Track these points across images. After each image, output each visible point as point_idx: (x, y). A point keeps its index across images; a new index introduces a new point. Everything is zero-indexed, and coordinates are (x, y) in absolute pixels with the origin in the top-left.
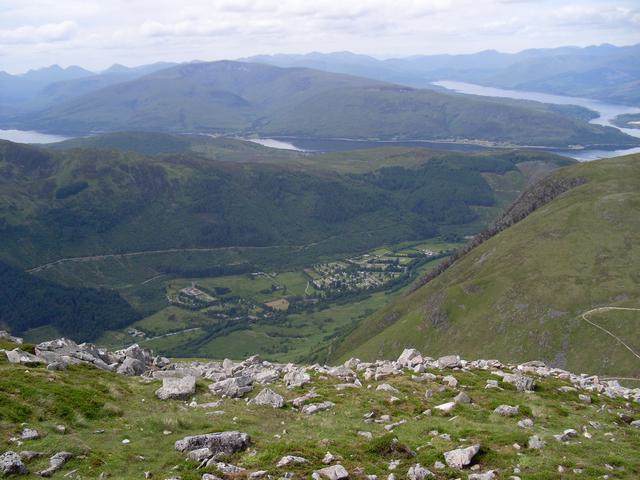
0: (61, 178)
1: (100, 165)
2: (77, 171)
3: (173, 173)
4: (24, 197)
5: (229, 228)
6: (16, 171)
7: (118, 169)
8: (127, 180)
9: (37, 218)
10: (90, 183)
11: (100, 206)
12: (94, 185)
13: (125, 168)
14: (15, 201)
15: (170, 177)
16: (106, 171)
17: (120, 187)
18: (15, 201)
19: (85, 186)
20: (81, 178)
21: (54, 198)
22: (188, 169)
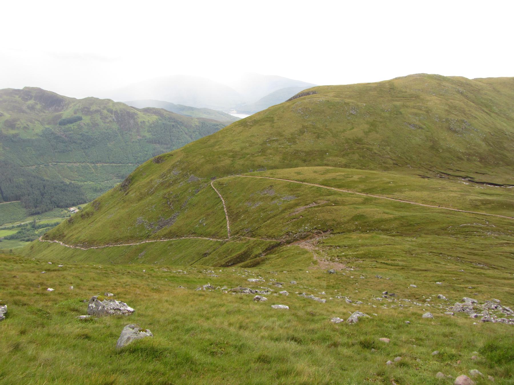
0: (67, 113)
1: (94, 108)
2: (78, 110)
3: (142, 117)
4: (36, 122)
6: (38, 107)
7: (105, 112)
8: (110, 119)
9: (41, 136)
10: (83, 118)
11: (87, 132)
12: (86, 119)
13: (110, 111)
14: (29, 123)
15: (140, 120)
16: (97, 111)
17: (105, 123)
18: (29, 123)
19: (80, 119)
20: (79, 114)
21: (58, 125)
22: (155, 116)
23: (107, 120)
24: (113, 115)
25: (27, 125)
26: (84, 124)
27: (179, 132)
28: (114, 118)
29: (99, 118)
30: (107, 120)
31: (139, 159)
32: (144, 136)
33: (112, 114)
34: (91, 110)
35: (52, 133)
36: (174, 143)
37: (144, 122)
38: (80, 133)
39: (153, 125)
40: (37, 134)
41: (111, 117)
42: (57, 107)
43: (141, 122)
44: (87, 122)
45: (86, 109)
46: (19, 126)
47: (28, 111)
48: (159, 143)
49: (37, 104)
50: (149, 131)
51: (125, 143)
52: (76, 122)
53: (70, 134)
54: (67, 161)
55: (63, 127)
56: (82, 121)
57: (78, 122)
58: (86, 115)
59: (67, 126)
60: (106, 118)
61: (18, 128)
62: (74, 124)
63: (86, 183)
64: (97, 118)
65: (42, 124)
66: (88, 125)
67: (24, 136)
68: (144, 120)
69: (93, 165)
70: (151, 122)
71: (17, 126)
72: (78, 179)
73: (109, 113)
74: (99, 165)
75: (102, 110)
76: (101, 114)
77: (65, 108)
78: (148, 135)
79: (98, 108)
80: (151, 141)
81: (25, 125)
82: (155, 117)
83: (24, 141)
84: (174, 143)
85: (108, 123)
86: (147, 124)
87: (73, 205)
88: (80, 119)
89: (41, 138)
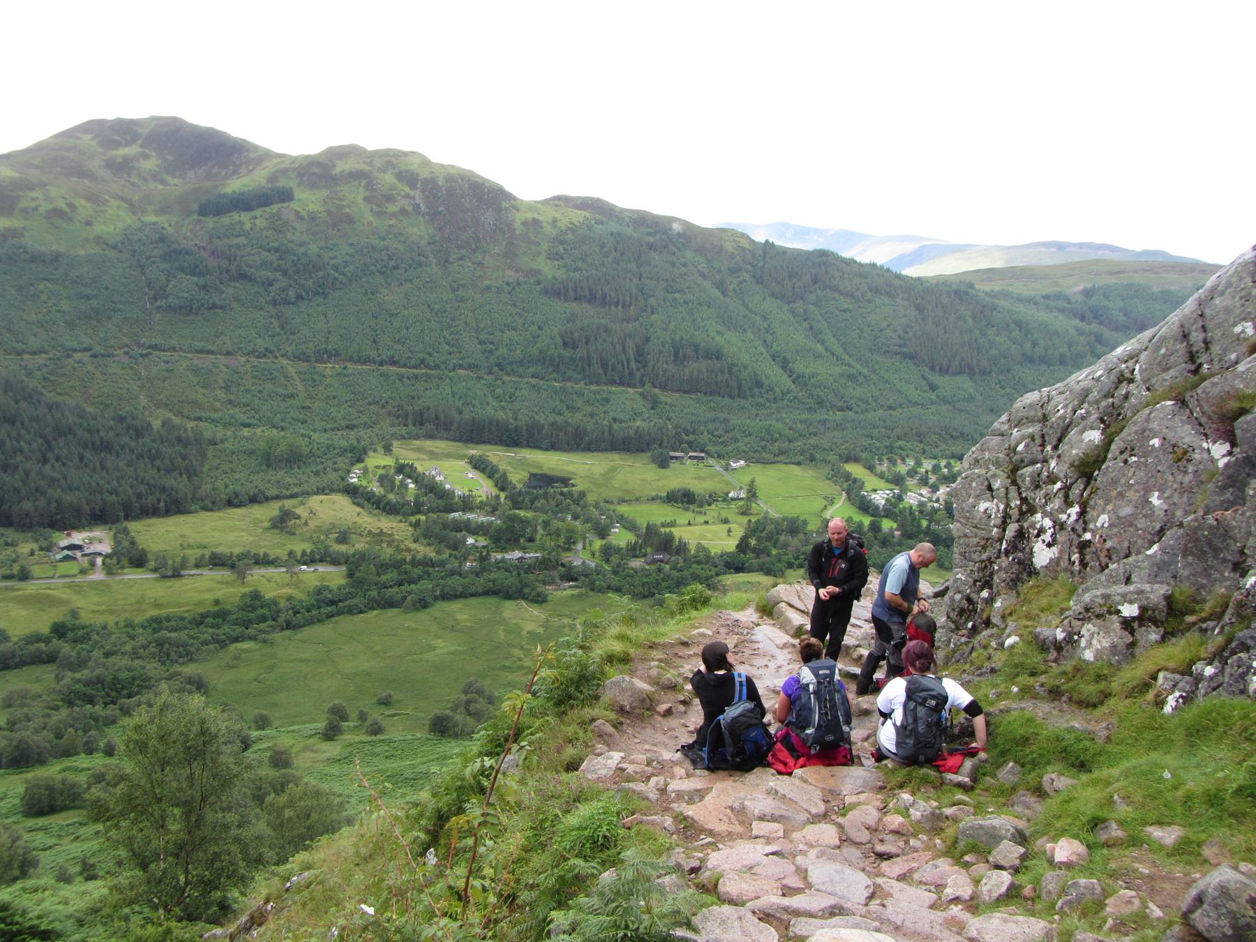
1: (343, 167)
5: (647, 340)
7: (389, 178)
9: (114, 247)
10: (298, 195)
13: (409, 178)
14: (81, 202)
16: (356, 176)
17: (379, 214)
18: (81, 202)
23: (392, 208)
24: (417, 193)
25: (72, 206)
26: (297, 213)
27: (673, 264)
28: (418, 201)
29: (360, 198)
30: (392, 208)
31: (503, 351)
32: (532, 272)
33: (413, 187)
34: (337, 171)
35: (162, 240)
36: (652, 301)
37: (535, 221)
38: (275, 245)
39: (570, 236)
40: (98, 240)
41: (407, 196)
42: (215, 170)
43: (525, 223)
44: (312, 207)
45: (315, 170)
46: (33, 204)
47: (107, 175)
48: (592, 298)
49: (145, 157)
50: (553, 256)
51: (453, 290)
52: (266, 204)
53: (238, 246)
54: (198, 345)
55: (210, 223)
56: (293, 205)
57: (275, 208)
58: (313, 186)
59: (226, 220)
60: (389, 198)
61: (24, 210)
62: (258, 212)
63: (246, 432)
64: (355, 197)
65: (133, 208)
66: (313, 218)
67: (41, 239)
68: (536, 216)
69: (303, 366)
70: (563, 224)
71: (24, 204)
72: (215, 416)
73: (399, 185)
74: (328, 368)
75: (375, 174)
76: (370, 186)
77: (243, 170)
78: (548, 270)
79: (367, 168)
80: (557, 292)
81: (61, 204)
82: (579, 216)
83: (35, 258)
84: (652, 301)
85: (393, 215)
86: (548, 229)
87: (100, 517)
88: (286, 196)
89: (111, 253)
